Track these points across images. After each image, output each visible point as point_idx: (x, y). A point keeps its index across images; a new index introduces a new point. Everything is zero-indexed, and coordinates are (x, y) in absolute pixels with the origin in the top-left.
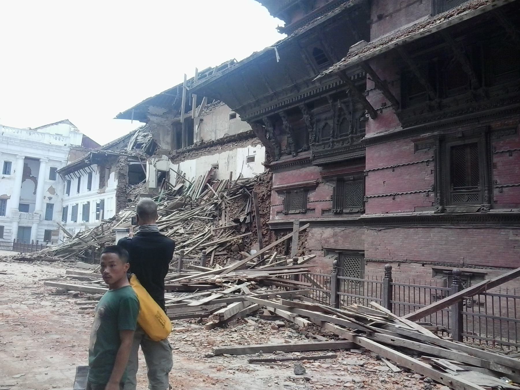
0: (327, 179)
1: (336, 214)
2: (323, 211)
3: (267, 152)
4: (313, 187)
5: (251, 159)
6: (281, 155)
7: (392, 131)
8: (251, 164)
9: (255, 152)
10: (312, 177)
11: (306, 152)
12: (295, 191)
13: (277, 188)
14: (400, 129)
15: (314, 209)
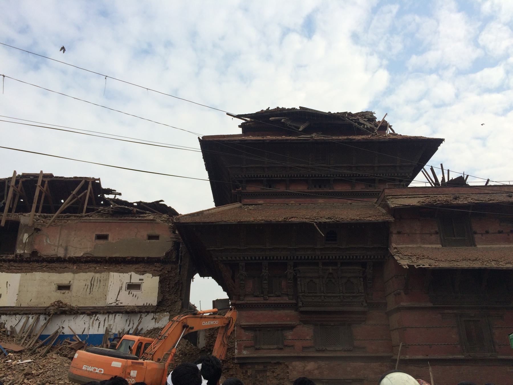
0: (305, 322)
1: (318, 351)
2: (304, 348)
3: (160, 282)
4: (291, 328)
5: (132, 287)
6: (246, 295)
7: (423, 305)
8: (135, 292)
9: (140, 280)
10: (288, 319)
11: (279, 298)
12: (269, 329)
13: (244, 325)
14: (430, 305)
15: (292, 346)
